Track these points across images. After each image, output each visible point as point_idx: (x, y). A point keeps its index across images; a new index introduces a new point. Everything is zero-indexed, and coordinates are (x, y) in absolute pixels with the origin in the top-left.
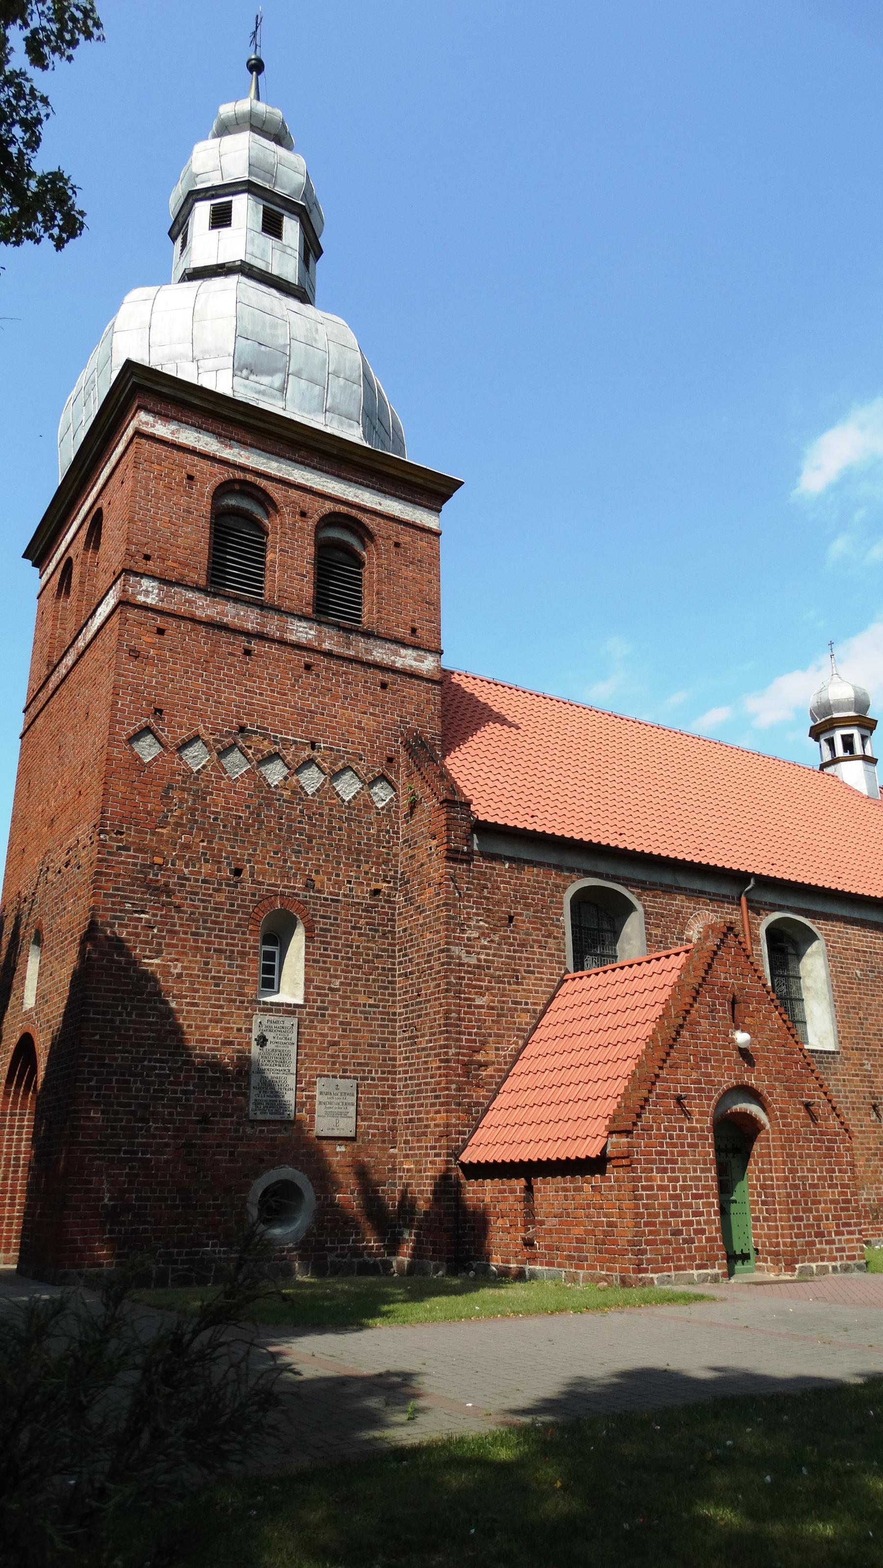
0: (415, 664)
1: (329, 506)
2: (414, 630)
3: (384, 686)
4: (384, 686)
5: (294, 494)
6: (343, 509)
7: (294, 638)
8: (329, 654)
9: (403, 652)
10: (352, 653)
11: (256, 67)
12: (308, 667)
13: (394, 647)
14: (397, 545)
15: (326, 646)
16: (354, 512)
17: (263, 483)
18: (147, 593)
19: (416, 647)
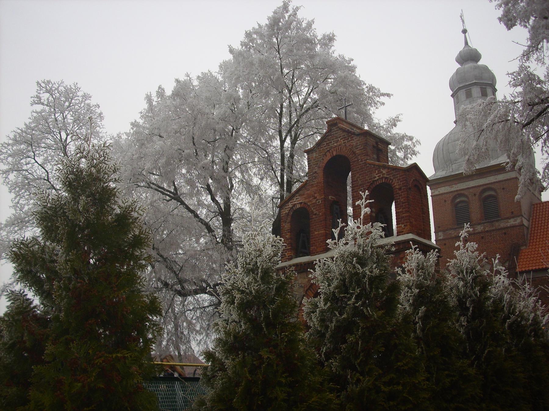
0: (514, 223)
1: (481, 188)
2: (512, 213)
3: (505, 234)
4: (505, 234)
5: (471, 190)
6: (485, 187)
7: (477, 231)
8: (487, 231)
9: (509, 221)
10: (494, 228)
11: (465, 31)
12: (482, 238)
13: (506, 221)
14: (503, 189)
15: (487, 229)
16: (488, 186)
17: (462, 192)
18: (440, 236)
19: (513, 217)
